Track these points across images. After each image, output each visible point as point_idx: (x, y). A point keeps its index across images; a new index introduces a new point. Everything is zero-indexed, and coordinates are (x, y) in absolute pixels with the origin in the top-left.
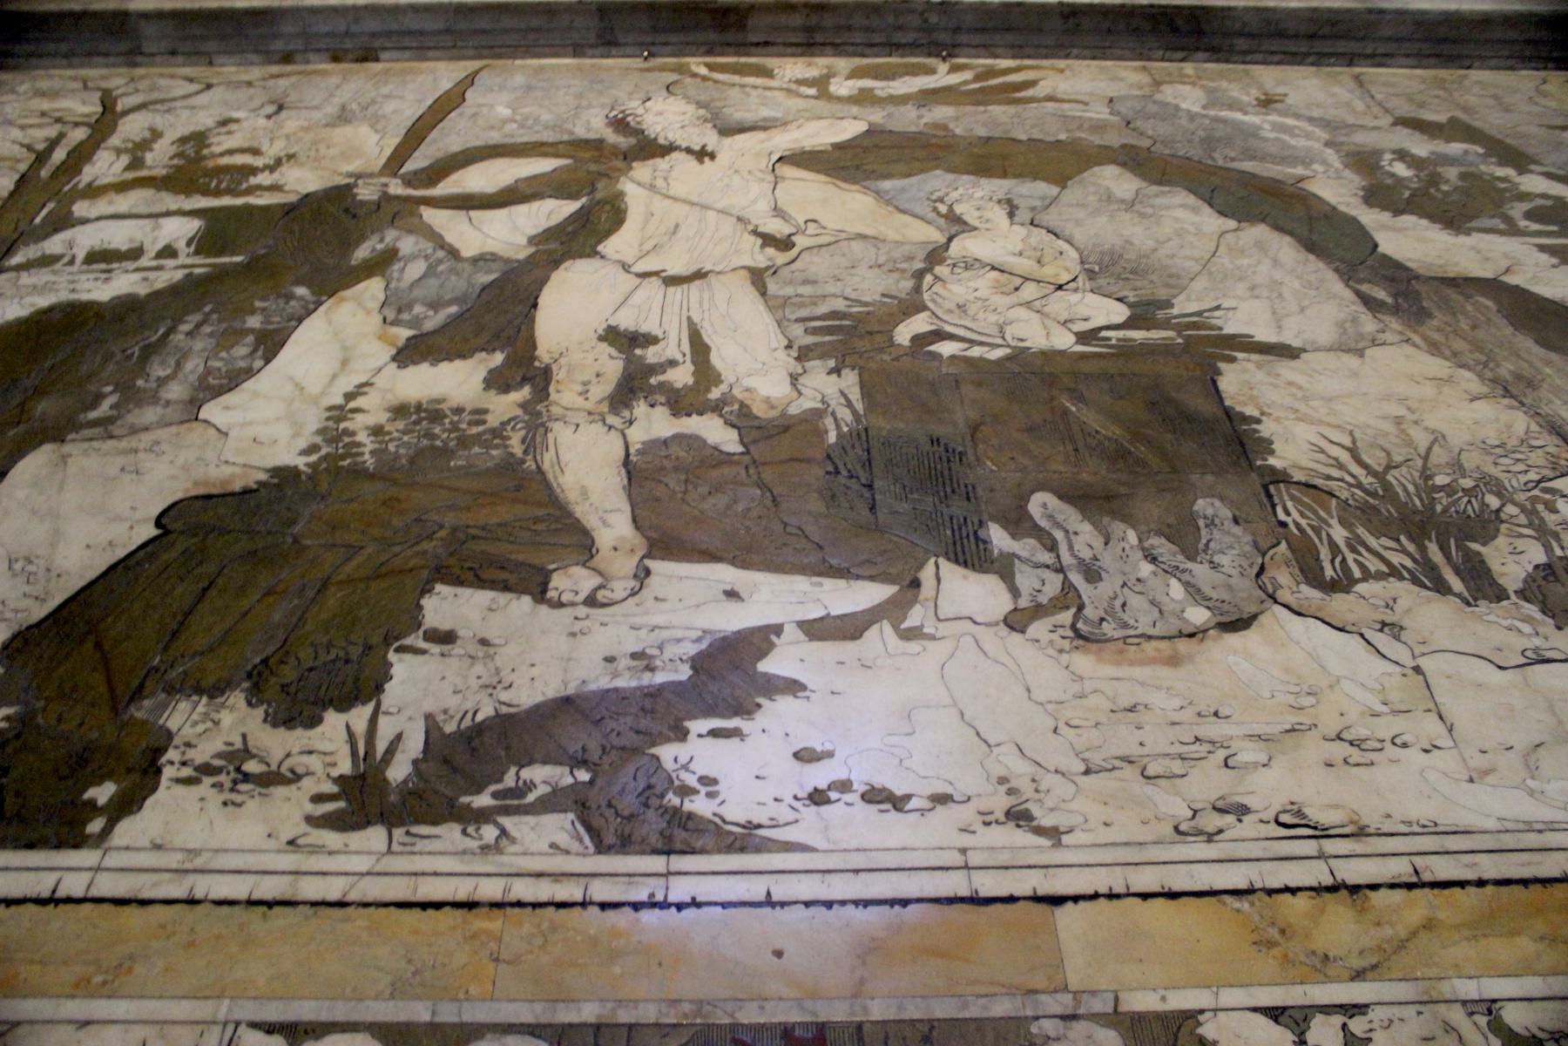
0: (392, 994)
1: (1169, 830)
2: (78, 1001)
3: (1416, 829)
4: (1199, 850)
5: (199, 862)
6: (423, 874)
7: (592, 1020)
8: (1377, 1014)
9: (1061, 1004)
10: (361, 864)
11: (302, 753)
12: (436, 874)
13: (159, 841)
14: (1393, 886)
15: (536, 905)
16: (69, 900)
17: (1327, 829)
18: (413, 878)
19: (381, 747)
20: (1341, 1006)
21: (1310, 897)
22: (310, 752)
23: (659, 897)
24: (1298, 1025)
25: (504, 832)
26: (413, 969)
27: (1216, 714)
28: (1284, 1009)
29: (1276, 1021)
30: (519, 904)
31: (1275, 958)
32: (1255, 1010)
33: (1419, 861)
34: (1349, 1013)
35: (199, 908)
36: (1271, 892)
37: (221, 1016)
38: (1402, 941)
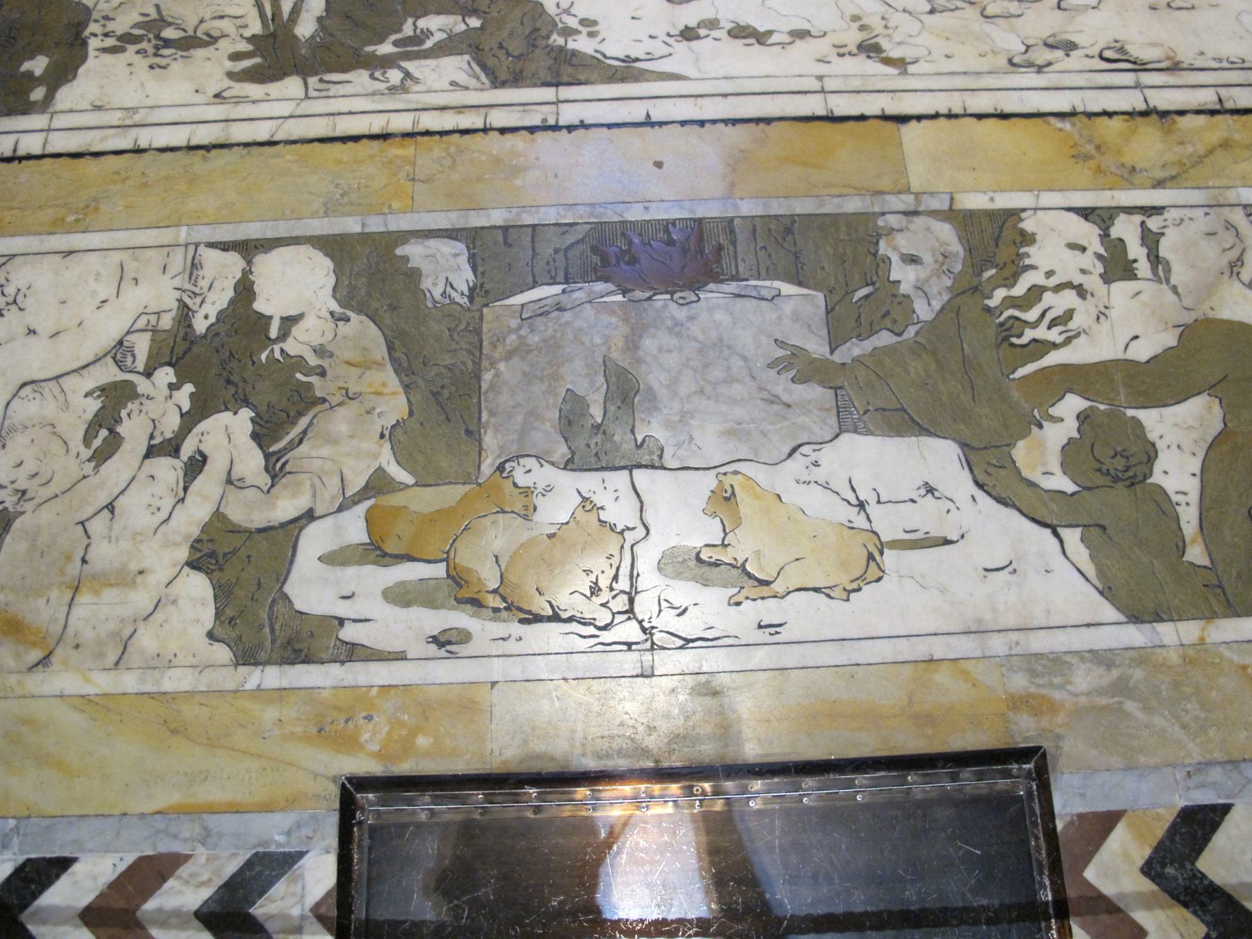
0: (325, 212)
1: (1003, 61)
2: (58, 236)
3: (1225, 65)
4: (1031, 79)
5: (137, 118)
6: (340, 114)
7: (500, 223)
8: (1171, 215)
9: (903, 202)
10: (284, 109)
11: (215, 18)
12: (351, 113)
13: (98, 103)
14: (1198, 112)
15: (442, 133)
16: (29, 157)
17: (1145, 64)
18: (331, 118)
19: (286, 15)
21: (1124, 120)
22: (222, 17)
23: (551, 122)
24: (1104, 222)
25: (408, 74)
26: (341, 192)
28: (1094, 209)
30: (428, 133)
31: (1090, 169)
32: (1069, 209)
33: (1224, 92)
34: (1148, 214)
35: (146, 155)
36: (1090, 115)
37: (182, 240)
38: (1200, 157)
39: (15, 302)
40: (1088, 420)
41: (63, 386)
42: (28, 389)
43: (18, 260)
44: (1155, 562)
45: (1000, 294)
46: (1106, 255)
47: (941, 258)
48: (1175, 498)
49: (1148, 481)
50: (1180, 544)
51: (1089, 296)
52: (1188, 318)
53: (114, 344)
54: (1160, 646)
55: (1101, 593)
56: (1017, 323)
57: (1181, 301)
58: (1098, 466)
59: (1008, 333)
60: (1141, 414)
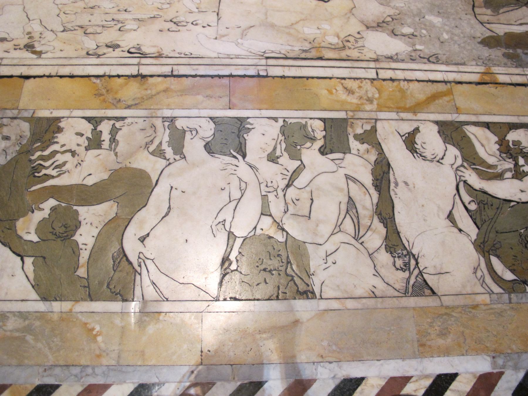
1: (84, 52)
3: (183, 56)
4: (93, 60)
14: (159, 76)
17: (147, 55)
20: (116, 118)
21: (125, 79)
27: (125, 11)
29: (89, 122)
31: (100, 100)
33: (175, 67)
34: (118, 120)
36: (110, 76)
38: (152, 95)
40: (55, 210)
44: (62, 275)
45: (39, 153)
46: (91, 138)
47: (19, 137)
48: (81, 246)
49: (72, 238)
50: (76, 267)
51: (76, 156)
52: (117, 167)
54: (51, 312)
55: (33, 287)
56: (41, 167)
57: (117, 159)
58: (52, 230)
59: (35, 171)
60: (79, 209)
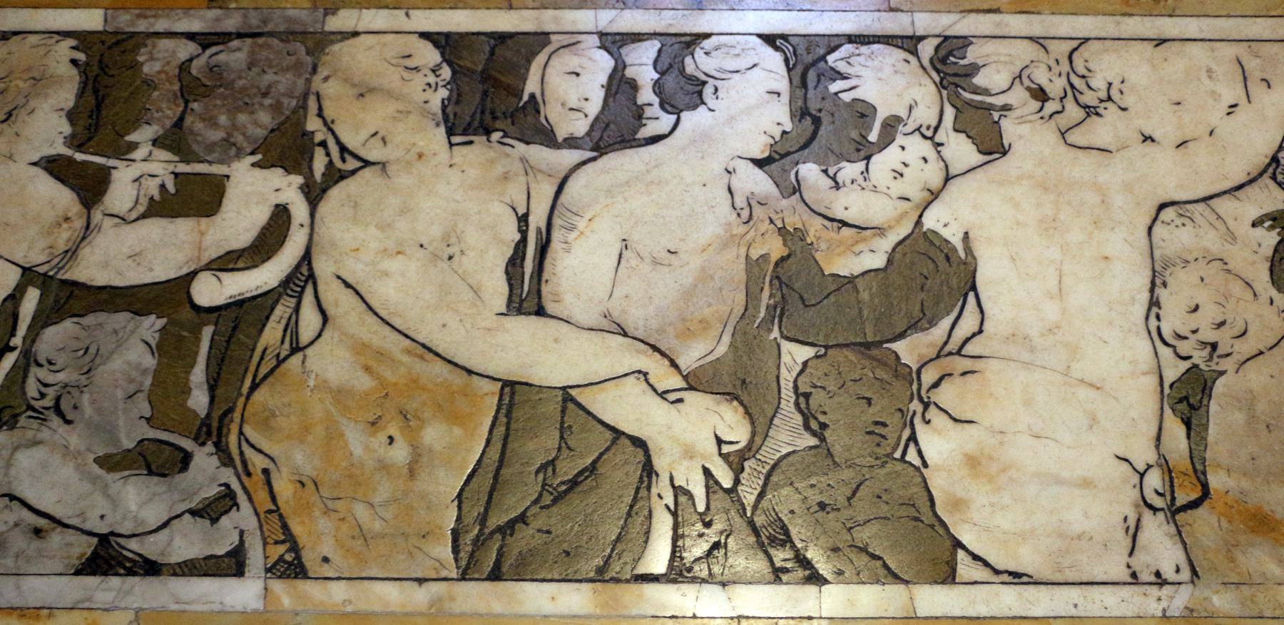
39: (1109, 99)
41: (1218, 211)
42: (1168, 214)
43: (1094, 45)
53: (1267, 161)
